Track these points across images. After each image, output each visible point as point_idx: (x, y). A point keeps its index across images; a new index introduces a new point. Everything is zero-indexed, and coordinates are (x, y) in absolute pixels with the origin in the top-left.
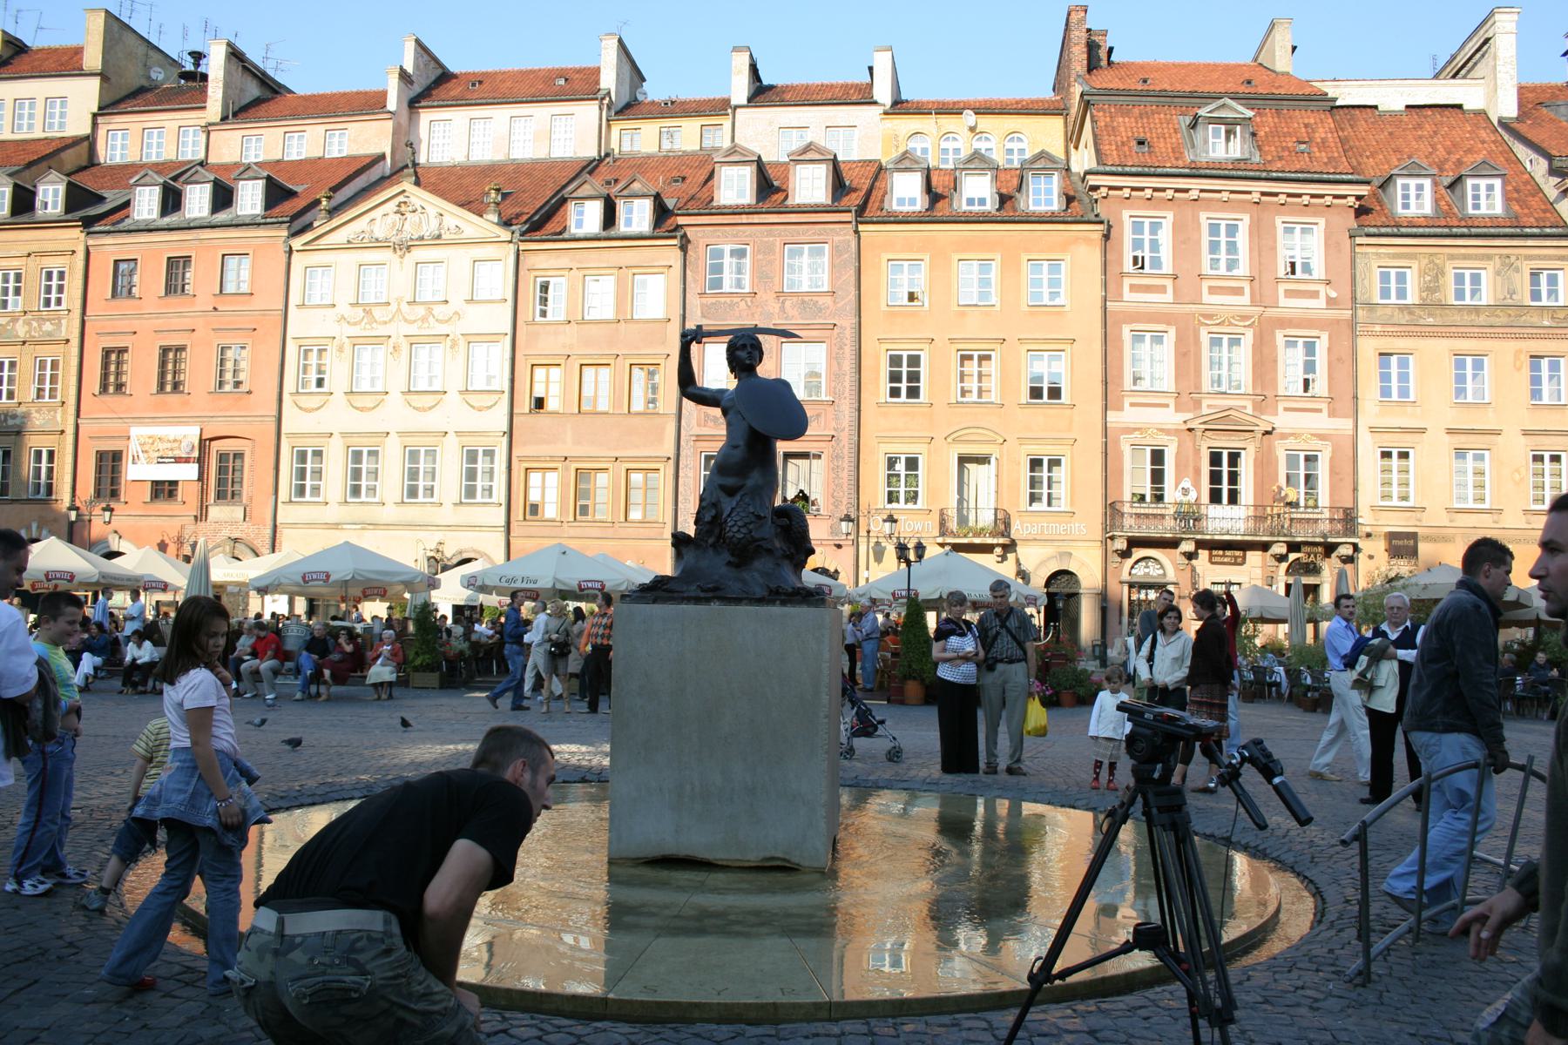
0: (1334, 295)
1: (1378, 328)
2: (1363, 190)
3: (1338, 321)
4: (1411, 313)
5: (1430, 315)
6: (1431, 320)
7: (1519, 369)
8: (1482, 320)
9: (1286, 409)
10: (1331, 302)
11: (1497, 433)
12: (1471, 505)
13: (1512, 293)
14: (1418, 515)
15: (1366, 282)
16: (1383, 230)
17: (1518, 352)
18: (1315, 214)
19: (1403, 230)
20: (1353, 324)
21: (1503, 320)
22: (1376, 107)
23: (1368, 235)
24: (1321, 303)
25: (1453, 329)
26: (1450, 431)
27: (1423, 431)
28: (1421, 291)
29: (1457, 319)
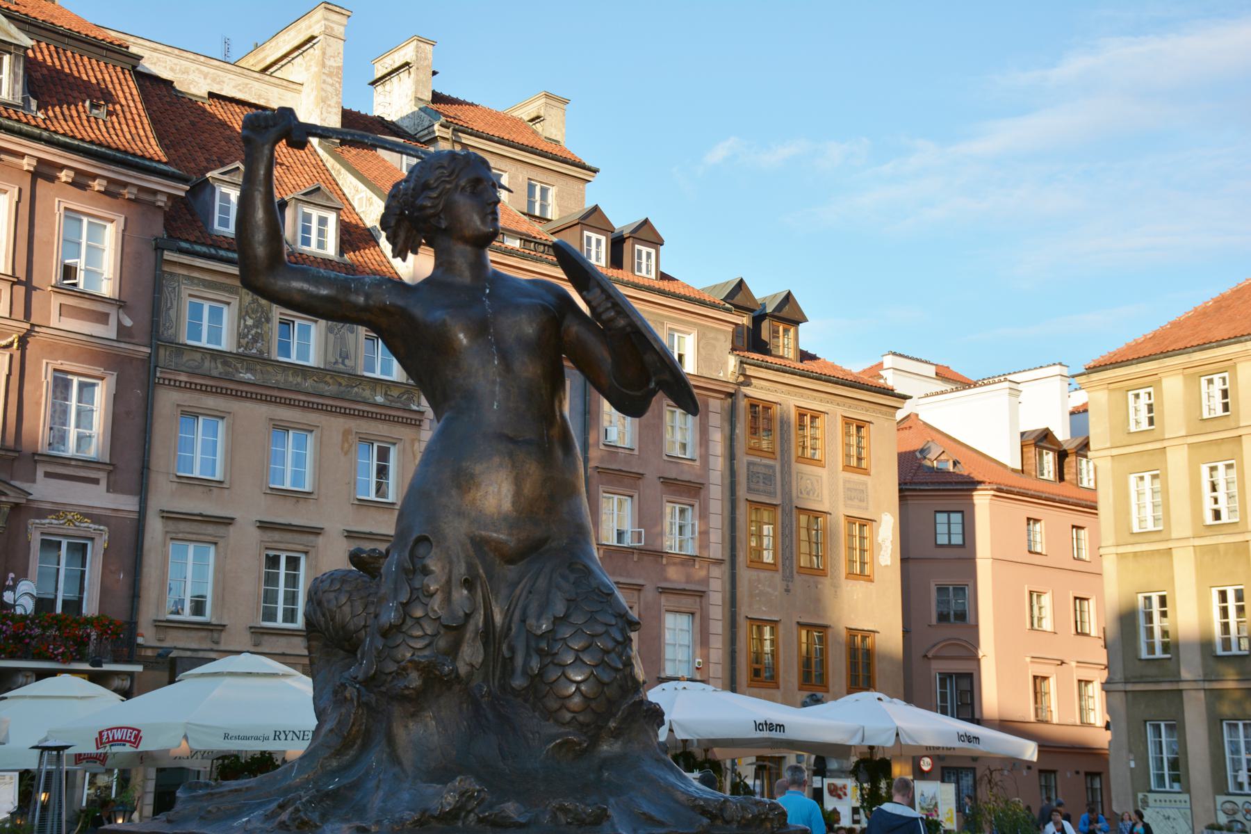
0: (128, 322)
1: (183, 378)
2: (180, 190)
3: (131, 359)
4: (225, 363)
5: (248, 370)
6: (248, 376)
7: (346, 454)
8: (308, 384)
9: (48, 475)
10: (121, 328)
11: (316, 532)
12: (280, 623)
13: (345, 356)
14: (215, 635)
15: (172, 313)
16: (198, 248)
17: (346, 433)
18: (110, 208)
19: (222, 253)
20: (150, 364)
21: (331, 389)
22: (169, 84)
23: (182, 251)
24: (109, 331)
25: (276, 393)
26: (264, 526)
27: (228, 522)
28: (241, 336)
29: (279, 378)
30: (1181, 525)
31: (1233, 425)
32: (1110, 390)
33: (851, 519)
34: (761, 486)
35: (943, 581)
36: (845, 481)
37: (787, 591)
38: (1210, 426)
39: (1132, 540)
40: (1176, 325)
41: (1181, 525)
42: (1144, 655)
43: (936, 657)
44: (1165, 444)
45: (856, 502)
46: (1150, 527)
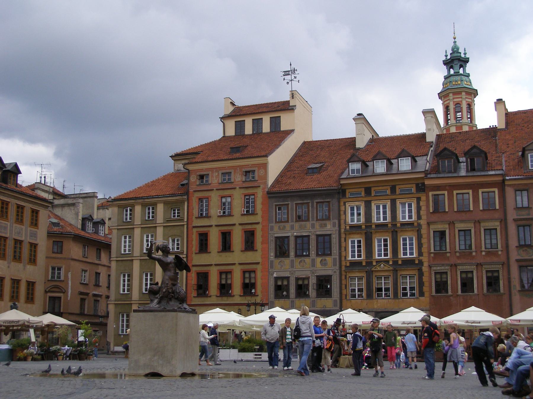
30: (137, 253)
31: (154, 222)
32: (119, 206)
33: (31, 244)
34: (3, 231)
35: (55, 265)
36: (30, 230)
37: (9, 267)
38: (147, 222)
39: (122, 256)
40: (140, 188)
41: (137, 253)
42: (122, 292)
43: (49, 291)
44: (134, 226)
45: (33, 238)
46: (127, 252)
